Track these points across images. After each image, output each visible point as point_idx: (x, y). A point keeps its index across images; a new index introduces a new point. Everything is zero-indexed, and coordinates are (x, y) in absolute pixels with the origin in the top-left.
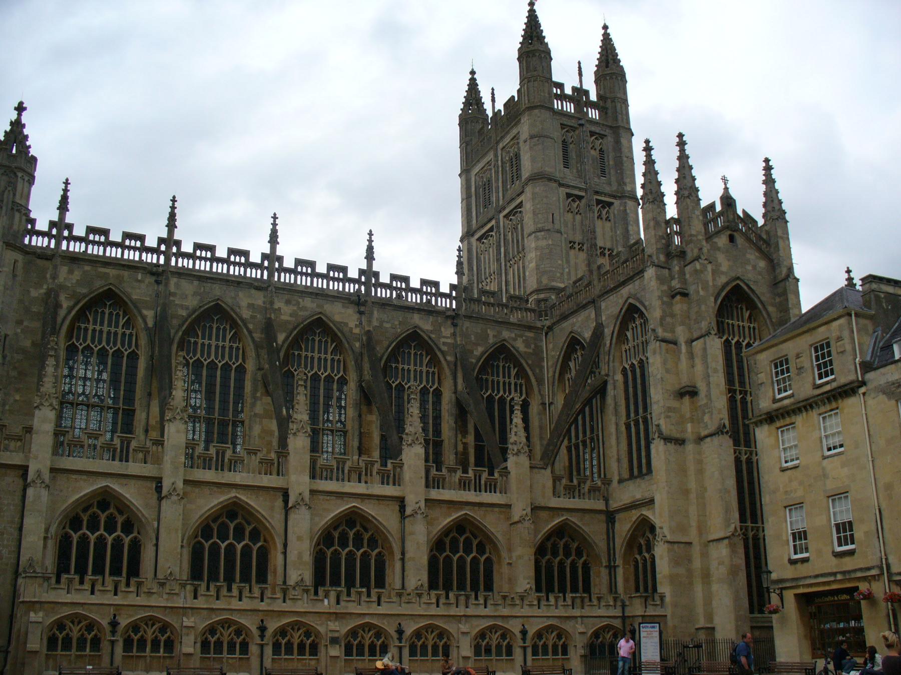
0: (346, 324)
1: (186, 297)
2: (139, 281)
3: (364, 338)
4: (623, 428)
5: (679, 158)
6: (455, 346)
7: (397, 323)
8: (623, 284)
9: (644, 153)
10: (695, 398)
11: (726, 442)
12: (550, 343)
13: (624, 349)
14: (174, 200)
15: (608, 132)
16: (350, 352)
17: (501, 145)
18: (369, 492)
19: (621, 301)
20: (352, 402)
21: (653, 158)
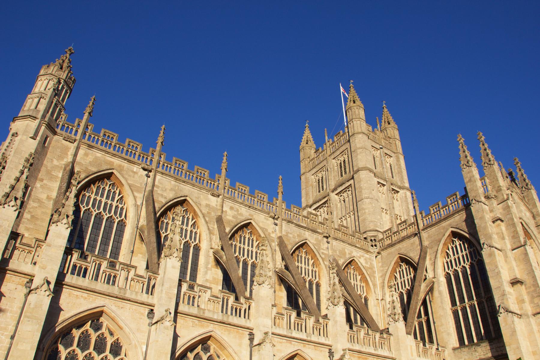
0: (267, 230)
1: (166, 190)
2: (135, 173)
6: (328, 255)
7: (296, 235)
12: (379, 262)
13: (445, 261)
15: (393, 155)
18: (309, 339)
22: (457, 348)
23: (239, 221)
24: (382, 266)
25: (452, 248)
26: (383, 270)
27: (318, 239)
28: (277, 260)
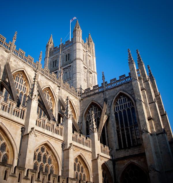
0: (31, 77)
7: (45, 82)
13: (115, 106)
18: (53, 135)
24: (82, 106)
25: (119, 100)
27: (55, 86)
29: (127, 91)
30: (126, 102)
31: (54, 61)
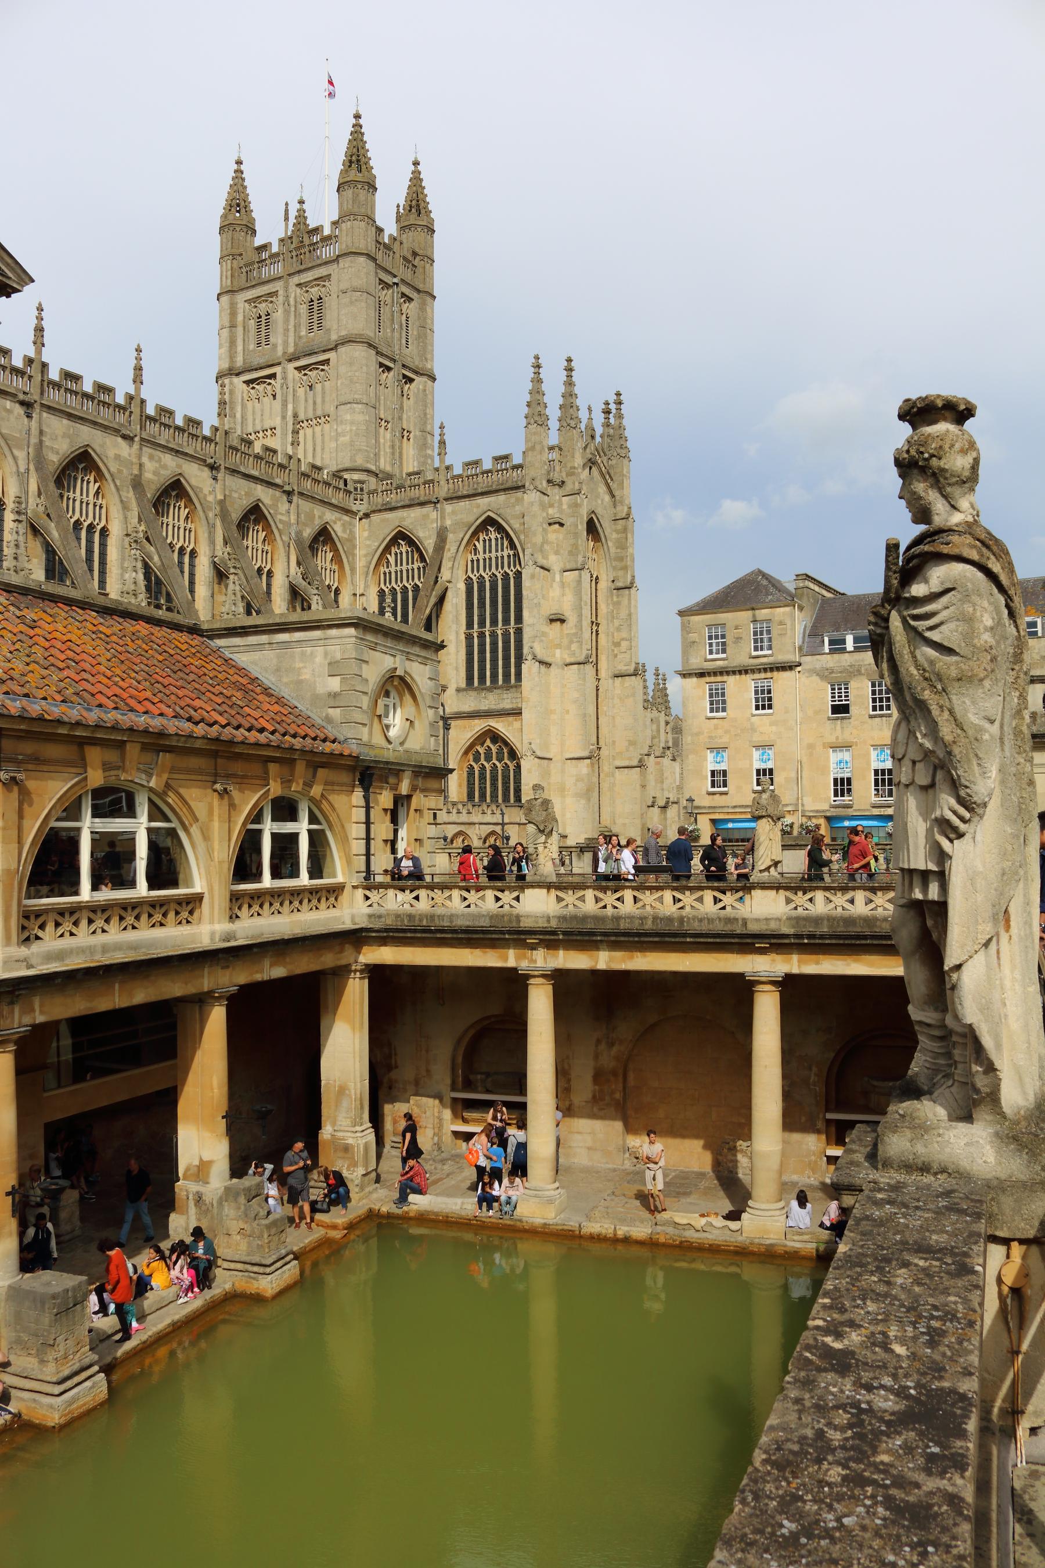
0: (201, 489)
3: (218, 508)
4: (463, 637)
5: (565, 383)
7: (243, 493)
8: (483, 494)
9: (533, 370)
10: (565, 625)
11: (589, 669)
13: (470, 559)
14: (40, 309)
16: (204, 522)
17: (296, 279)
19: (477, 512)
20: (203, 579)
21: (541, 376)
22: (464, 690)
23: (162, 480)
24: (368, 538)
25: (484, 541)
26: (369, 546)
28: (217, 542)
29: (509, 518)
30: (502, 550)
31: (260, 317)
